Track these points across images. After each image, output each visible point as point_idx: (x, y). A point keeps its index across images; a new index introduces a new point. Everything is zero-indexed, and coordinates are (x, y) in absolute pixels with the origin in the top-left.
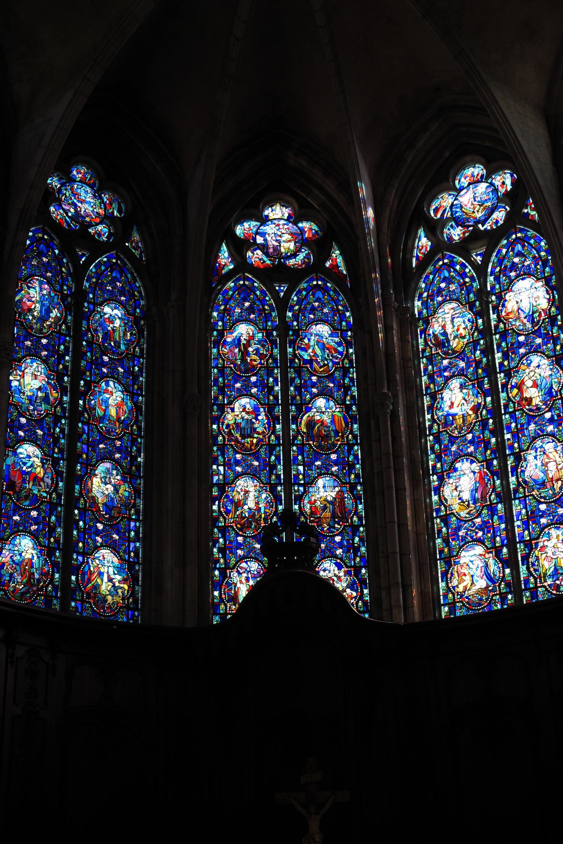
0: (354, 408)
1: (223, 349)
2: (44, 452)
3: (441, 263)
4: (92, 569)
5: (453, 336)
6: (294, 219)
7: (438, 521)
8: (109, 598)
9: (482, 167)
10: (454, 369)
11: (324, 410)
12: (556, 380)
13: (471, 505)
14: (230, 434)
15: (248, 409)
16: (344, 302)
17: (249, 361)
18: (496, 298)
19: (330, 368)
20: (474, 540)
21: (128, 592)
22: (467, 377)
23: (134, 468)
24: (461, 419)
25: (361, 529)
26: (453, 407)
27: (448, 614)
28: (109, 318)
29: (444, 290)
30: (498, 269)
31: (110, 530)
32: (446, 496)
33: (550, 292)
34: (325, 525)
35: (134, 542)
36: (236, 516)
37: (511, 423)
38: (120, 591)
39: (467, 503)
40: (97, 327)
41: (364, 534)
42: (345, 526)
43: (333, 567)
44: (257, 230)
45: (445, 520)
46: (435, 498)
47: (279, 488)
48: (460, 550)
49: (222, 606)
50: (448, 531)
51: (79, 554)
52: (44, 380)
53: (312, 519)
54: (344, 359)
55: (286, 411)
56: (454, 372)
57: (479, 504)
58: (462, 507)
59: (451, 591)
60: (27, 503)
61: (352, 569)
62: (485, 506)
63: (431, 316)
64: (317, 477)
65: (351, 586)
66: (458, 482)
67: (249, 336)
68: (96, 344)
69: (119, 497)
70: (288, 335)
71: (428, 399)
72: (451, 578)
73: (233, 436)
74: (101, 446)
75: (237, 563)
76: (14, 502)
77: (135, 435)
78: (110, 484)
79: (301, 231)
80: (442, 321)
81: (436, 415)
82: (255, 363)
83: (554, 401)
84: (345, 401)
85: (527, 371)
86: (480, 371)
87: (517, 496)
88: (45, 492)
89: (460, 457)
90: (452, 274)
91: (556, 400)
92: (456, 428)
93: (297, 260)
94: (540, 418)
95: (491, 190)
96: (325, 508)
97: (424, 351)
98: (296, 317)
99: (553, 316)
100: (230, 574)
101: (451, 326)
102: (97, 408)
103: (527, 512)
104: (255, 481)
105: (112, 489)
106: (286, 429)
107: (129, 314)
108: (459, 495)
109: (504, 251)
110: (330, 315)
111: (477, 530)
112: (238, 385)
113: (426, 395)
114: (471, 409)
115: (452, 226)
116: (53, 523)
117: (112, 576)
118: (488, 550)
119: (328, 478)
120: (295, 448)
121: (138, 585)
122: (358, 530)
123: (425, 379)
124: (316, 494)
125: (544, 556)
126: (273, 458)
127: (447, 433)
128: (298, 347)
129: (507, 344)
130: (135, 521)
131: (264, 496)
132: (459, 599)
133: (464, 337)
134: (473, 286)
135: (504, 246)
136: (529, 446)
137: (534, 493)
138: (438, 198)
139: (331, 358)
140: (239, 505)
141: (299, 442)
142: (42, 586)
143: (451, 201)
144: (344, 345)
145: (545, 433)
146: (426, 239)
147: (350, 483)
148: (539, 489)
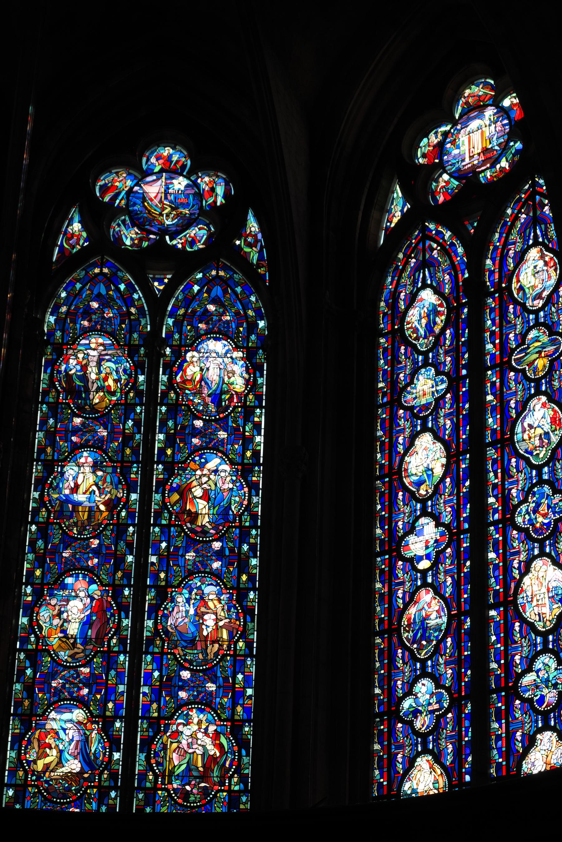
3: (97, 270)
5: (95, 386)
7: (22, 656)
9: (186, 153)
10: (88, 436)
12: (237, 499)
13: (79, 646)
18: (172, 352)
20: (73, 699)
22: (107, 455)
24: (86, 514)
26: (77, 493)
27: (12, 801)
29: (95, 313)
30: (181, 312)
33: (251, 371)
37: (161, 542)
39: (72, 641)
46: (24, 620)
56: (87, 441)
57: (91, 647)
58: (63, 645)
59: (24, 767)
62: (100, 651)
63: (67, 344)
66: (64, 605)
71: (39, 468)
72: (26, 748)
80: (83, 358)
83: (229, 527)
85: (199, 472)
86: (128, 451)
87: (151, 649)
90: (111, 293)
91: (232, 527)
92: (76, 524)
94: (205, 546)
95: (193, 192)
97: (46, 393)
99: (249, 406)
101: (95, 370)
103: (161, 676)
108: (62, 625)
109: (196, 288)
113: (38, 460)
114: (105, 503)
115: (124, 222)
118: (91, 718)
125: (175, 745)
127: (61, 528)
129: (176, 425)
132: (34, 781)
133: (113, 394)
134: (140, 322)
135: (198, 282)
136: (181, 582)
137: (176, 652)
138: (111, 172)
143: (129, 183)
145: (208, 570)
148: (186, 647)
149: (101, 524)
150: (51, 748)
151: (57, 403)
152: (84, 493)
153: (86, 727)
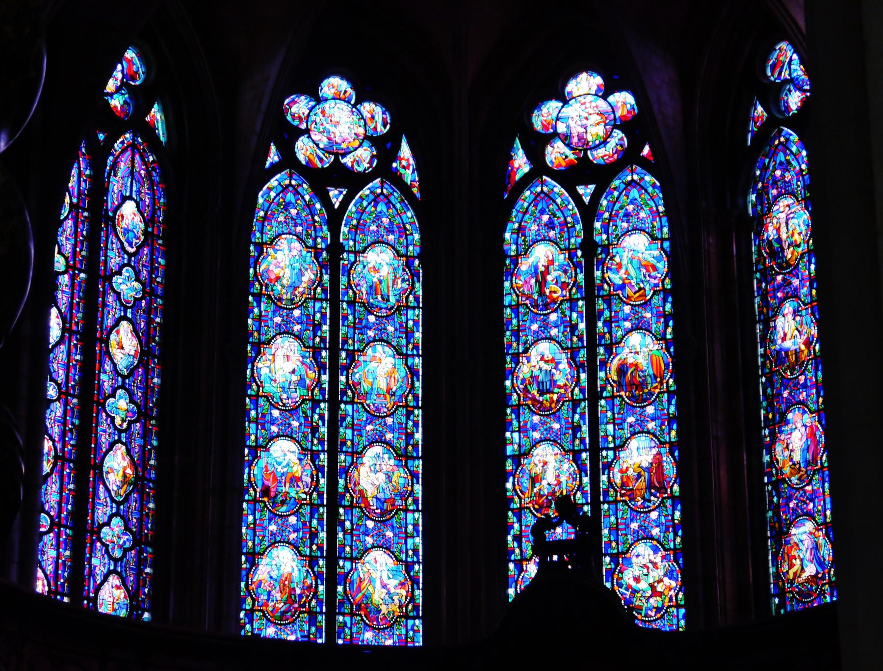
1: (517, 280)
2: (301, 446)
4: (362, 576)
6: (605, 92)
7: (770, 488)
8: (384, 609)
11: (638, 350)
13: (803, 469)
14: (526, 391)
17: (548, 294)
19: (647, 293)
23: (410, 448)
28: (374, 267)
29: (779, 181)
31: (382, 527)
32: (777, 456)
34: (639, 498)
35: (413, 537)
36: (533, 495)
38: (396, 598)
39: (798, 466)
42: (663, 498)
45: (776, 485)
46: (766, 458)
47: (584, 455)
51: (345, 559)
52: (299, 360)
53: (623, 492)
54: (665, 279)
58: (793, 471)
60: (284, 509)
64: (629, 438)
66: (789, 438)
67: (548, 261)
68: (358, 302)
73: (530, 393)
74: (369, 428)
76: (270, 511)
77: (411, 407)
80: (777, 223)
81: (769, 348)
82: (555, 295)
88: (305, 493)
96: (639, 476)
97: (758, 262)
98: (605, 228)
102: (363, 382)
104: (556, 449)
106: (592, 378)
107: (399, 255)
108: (790, 455)
110: (649, 220)
112: (535, 327)
113: (759, 322)
116: (315, 528)
117: (386, 581)
119: (643, 438)
120: (603, 402)
124: (628, 459)
126: (577, 417)
127: (780, 374)
128: (608, 268)
130: (413, 511)
133: (799, 246)
138: (776, 50)
139: (648, 278)
141: (608, 395)
142: (305, 602)
149: (804, 361)
150: (795, 559)
151: (765, 268)
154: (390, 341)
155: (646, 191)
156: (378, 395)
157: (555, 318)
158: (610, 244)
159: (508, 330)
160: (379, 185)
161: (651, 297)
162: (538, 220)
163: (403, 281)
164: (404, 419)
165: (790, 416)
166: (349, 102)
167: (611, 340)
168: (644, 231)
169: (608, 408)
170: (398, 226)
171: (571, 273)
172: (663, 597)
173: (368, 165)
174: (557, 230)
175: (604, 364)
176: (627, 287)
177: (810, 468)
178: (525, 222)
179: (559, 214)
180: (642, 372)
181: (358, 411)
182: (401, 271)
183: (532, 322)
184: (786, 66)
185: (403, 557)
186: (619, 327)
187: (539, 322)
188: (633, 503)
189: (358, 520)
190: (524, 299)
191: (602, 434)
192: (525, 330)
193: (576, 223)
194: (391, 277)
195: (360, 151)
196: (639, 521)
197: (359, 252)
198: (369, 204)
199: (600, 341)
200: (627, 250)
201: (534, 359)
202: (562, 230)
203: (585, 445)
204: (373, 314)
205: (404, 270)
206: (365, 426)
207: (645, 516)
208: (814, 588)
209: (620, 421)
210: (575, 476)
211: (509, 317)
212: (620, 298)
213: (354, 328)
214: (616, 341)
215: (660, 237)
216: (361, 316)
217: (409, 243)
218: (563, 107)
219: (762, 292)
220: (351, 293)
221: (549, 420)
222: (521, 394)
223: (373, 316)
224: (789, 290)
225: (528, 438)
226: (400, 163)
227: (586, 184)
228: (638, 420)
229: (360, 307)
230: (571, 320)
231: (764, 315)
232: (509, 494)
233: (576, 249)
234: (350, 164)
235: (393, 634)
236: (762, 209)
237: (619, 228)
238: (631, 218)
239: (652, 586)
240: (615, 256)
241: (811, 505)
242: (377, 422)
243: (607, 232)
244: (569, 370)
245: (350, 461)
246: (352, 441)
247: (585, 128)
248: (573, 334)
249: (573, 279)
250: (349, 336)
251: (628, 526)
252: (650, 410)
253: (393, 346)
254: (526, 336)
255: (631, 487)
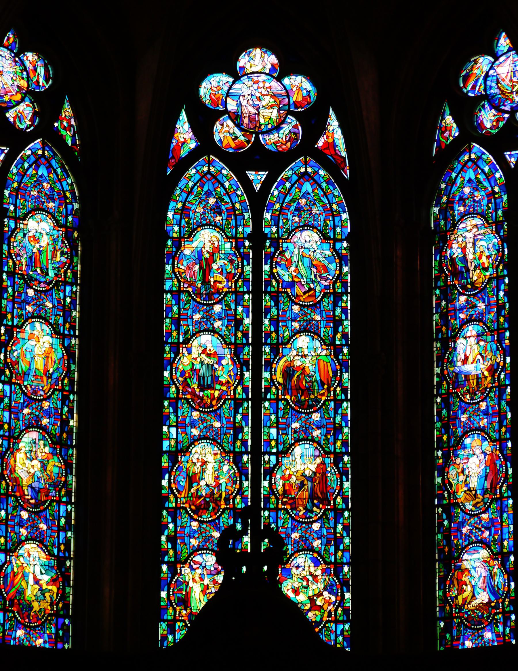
0: (345, 350)
1: (179, 265)
4: (15, 570)
5: (473, 265)
7: (440, 510)
8: (36, 605)
11: (306, 353)
13: (479, 496)
14: (186, 384)
15: (210, 350)
16: (340, 199)
17: (212, 283)
19: (317, 294)
20: (479, 542)
21: (57, 596)
22: (486, 326)
23: (65, 435)
24: (475, 381)
25: (346, 514)
26: (467, 364)
29: (468, 199)
31: (36, 519)
32: (451, 480)
34: (301, 508)
36: (190, 495)
38: (47, 595)
39: (474, 492)
40: (19, 250)
41: (350, 521)
42: (326, 510)
43: (309, 563)
44: (229, 90)
47: (245, 458)
48: (462, 552)
49: (171, 611)
50: (450, 525)
53: (285, 500)
55: (257, 354)
57: (488, 495)
58: (468, 497)
61: (332, 566)
64: (293, 444)
65: (329, 588)
66: (465, 463)
67: (214, 247)
68: (18, 274)
69: (47, 475)
70: (264, 247)
73: (190, 387)
74: (26, 411)
75: (189, 556)
77: (66, 391)
78: (36, 458)
79: (287, 91)
80: (463, 242)
81: (447, 369)
82: (219, 286)
84: (335, 340)
86: (502, 320)
89: (471, 431)
93: (280, 135)
96: (302, 485)
97: (438, 278)
98: (276, 220)
100: (181, 570)
102: (21, 362)
104: (216, 448)
105: (39, 465)
106: (257, 378)
108: (466, 481)
110: (322, 218)
111: (483, 529)
112: (197, 317)
113: (437, 340)
117: (39, 577)
118: (494, 556)
119: (307, 446)
120: (267, 404)
121: (69, 586)
122: (342, 515)
123: (436, 317)
126: (239, 417)
127: (458, 396)
130: (66, 504)
131: (226, 468)
133: (486, 269)
138: (470, 61)
139: (319, 279)
140: (192, 479)
144: (337, 261)
146: (450, 117)
147: (335, 453)
149: (487, 388)
150: (466, 585)
152: (472, 363)
153: (489, 564)
154: (48, 318)
155: (320, 186)
156: (35, 376)
157: (220, 310)
158: (279, 238)
159: (167, 317)
160: (39, 147)
161: (321, 300)
162: (203, 203)
163: (62, 254)
164: (59, 404)
165: (467, 441)
166: (11, 50)
167: (278, 339)
168: (316, 228)
169: (272, 411)
170: (58, 193)
171: (238, 263)
172: (322, 611)
173: (30, 123)
174: (224, 216)
175: (269, 364)
176: (296, 286)
177: (488, 496)
178: (189, 203)
179: (227, 199)
180: (309, 376)
181: (15, 392)
182: (60, 243)
183: (194, 312)
184: (481, 80)
185: (56, 551)
186: (286, 326)
187: (201, 313)
188: (295, 512)
189: (14, 509)
190: (186, 286)
191: (264, 437)
192: (186, 320)
193: (244, 211)
194: (51, 248)
195: (21, 107)
196: (300, 531)
197: (19, 219)
198: (30, 166)
199: (266, 340)
200: (297, 247)
201: (195, 352)
202: (229, 216)
203: (246, 447)
204: (32, 288)
205: (63, 242)
206: (22, 410)
207: (307, 527)
208: (485, 615)
209: (284, 426)
210: (235, 479)
211: (170, 303)
212: (288, 296)
213: (13, 302)
214: (282, 341)
215: (332, 237)
216: (21, 289)
217: (69, 213)
218: (234, 83)
219: (442, 311)
220: (11, 262)
221: (209, 418)
222: (181, 388)
223: (32, 290)
224: (473, 313)
225: (187, 434)
226: (62, 123)
227: (257, 170)
228: (303, 427)
229: (20, 279)
230: (235, 314)
231: (442, 334)
232: (164, 492)
233: (244, 238)
234: (12, 120)
235: (44, 633)
236: (445, 224)
237: (290, 222)
238: (303, 213)
239: (311, 600)
240: (285, 251)
241: (487, 533)
242: (34, 406)
243: (277, 225)
244: (232, 367)
245: (7, 446)
246: (9, 424)
247: (258, 109)
248: (237, 329)
249: (240, 271)
250: (8, 310)
251: (289, 536)
252: (316, 417)
253: (51, 324)
254: (188, 326)
255: (293, 496)
